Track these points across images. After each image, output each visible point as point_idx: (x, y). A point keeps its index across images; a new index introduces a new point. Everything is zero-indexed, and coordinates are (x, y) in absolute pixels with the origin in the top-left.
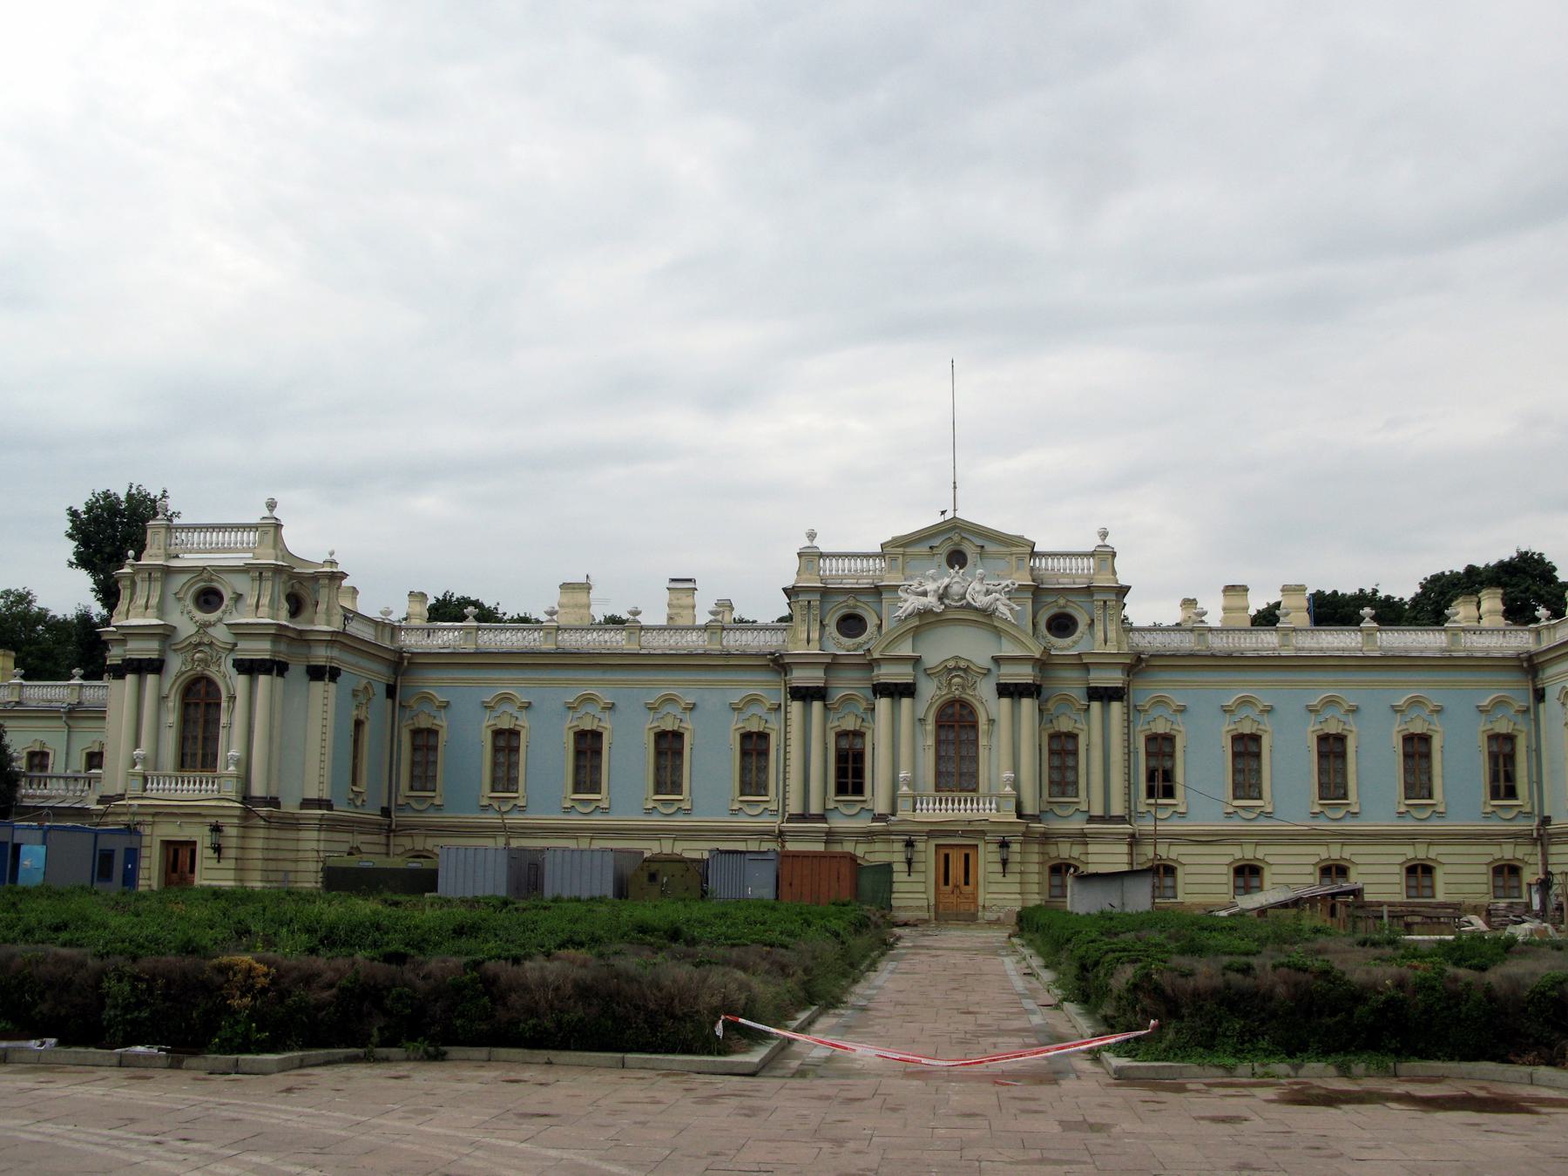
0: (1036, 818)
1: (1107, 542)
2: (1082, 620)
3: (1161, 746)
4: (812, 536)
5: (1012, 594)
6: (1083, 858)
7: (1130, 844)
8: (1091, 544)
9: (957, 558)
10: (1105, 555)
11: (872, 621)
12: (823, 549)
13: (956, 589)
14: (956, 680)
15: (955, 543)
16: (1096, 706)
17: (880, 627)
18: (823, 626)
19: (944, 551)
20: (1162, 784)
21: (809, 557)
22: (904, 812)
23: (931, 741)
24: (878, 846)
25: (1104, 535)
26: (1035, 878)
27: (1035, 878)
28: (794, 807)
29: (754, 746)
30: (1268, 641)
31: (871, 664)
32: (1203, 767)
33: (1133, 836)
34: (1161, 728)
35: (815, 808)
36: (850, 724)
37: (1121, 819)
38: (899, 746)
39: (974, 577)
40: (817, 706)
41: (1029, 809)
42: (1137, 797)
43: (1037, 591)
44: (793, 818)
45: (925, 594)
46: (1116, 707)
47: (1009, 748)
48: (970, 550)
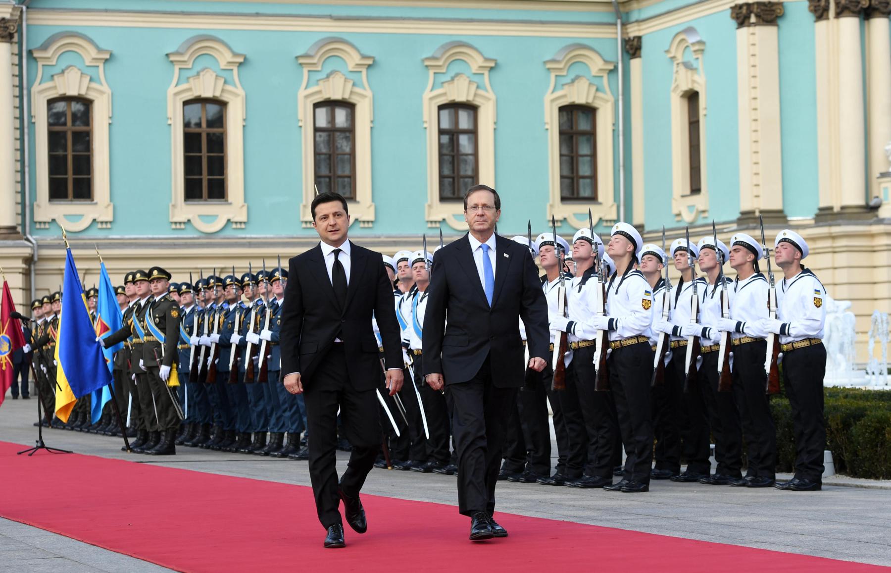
34: (71, 85)
42: (33, 197)
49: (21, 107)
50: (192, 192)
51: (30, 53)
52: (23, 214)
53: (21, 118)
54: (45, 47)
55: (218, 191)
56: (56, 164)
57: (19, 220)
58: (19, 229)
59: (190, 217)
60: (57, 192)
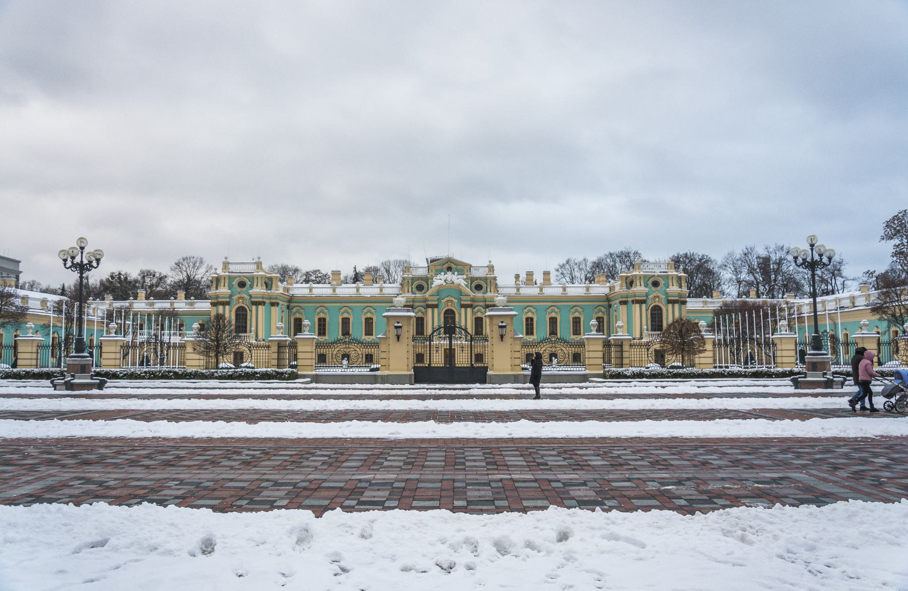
8: (487, 264)
9: (449, 269)
10: (491, 268)
11: (426, 286)
13: (449, 279)
15: (450, 265)
19: (446, 266)
31: (426, 300)
36: (420, 315)
43: (473, 279)
48: (453, 266)
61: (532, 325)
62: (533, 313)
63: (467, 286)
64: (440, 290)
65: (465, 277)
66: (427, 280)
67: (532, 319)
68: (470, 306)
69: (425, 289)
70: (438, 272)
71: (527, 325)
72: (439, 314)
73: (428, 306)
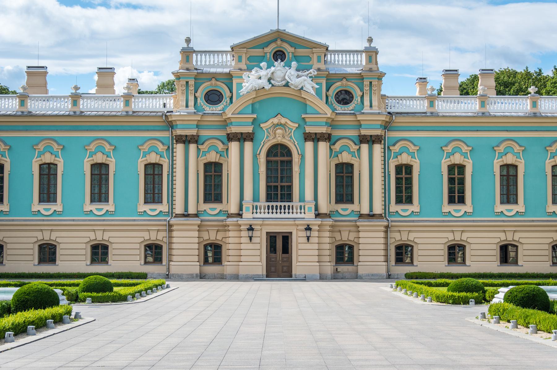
0: (327, 216)
1: (372, 45)
2: (357, 93)
3: (404, 173)
4: (188, 40)
5: (313, 78)
6: (356, 240)
7: (386, 232)
8: (362, 45)
9: (279, 55)
10: (372, 53)
12: (196, 49)
14: (279, 131)
15: (278, 46)
16: (365, 147)
17: (231, 98)
18: (196, 98)
19: (270, 49)
20: (404, 194)
21: (187, 53)
22: (247, 215)
23: (263, 169)
24: (231, 234)
25: (370, 40)
26: (327, 252)
27: (327, 252)
28: (179, 209)
29: (153, 172)
30: (470, 106)
32: (430, 183)
33: (387, 227)
34: (405, 159)
35: (192, 210)
37: (380, 216)
38: (244, 171)
39: (290, 67)
40: (193, 147)
41: (324, 209)
42: (389, 203)
44: (177, 216)
45: (260, 78)
46: (378, 148)
47: (313, 172)
48: (288, 49)
49: (385, 169)
50: (451, 200)
51: (388, 148)
52: (385, 209)
53: (385, 173)
54: (394, 145)
55: (462, 200)
56: (398, 189)
57: (383, 211)
58: (383, 215)
59: (450, 210)
60: (399, 201)
61: (462, 182)
62: (465, 155)
63: (318, 92)
64: (260, 101)
65: (313, 72)
66: (229, 78)
67: (461, 168)
68: (327, 137)
69: (226, 100)
70: (253, 62)
71: (451, 181)
72: (255, 157)
73: (231, 137)
